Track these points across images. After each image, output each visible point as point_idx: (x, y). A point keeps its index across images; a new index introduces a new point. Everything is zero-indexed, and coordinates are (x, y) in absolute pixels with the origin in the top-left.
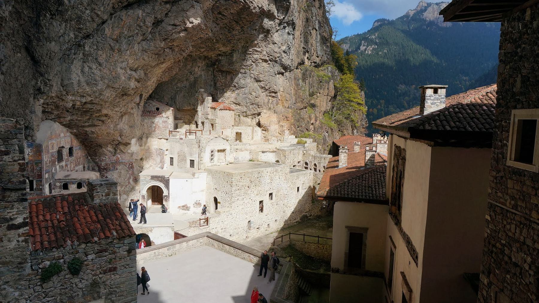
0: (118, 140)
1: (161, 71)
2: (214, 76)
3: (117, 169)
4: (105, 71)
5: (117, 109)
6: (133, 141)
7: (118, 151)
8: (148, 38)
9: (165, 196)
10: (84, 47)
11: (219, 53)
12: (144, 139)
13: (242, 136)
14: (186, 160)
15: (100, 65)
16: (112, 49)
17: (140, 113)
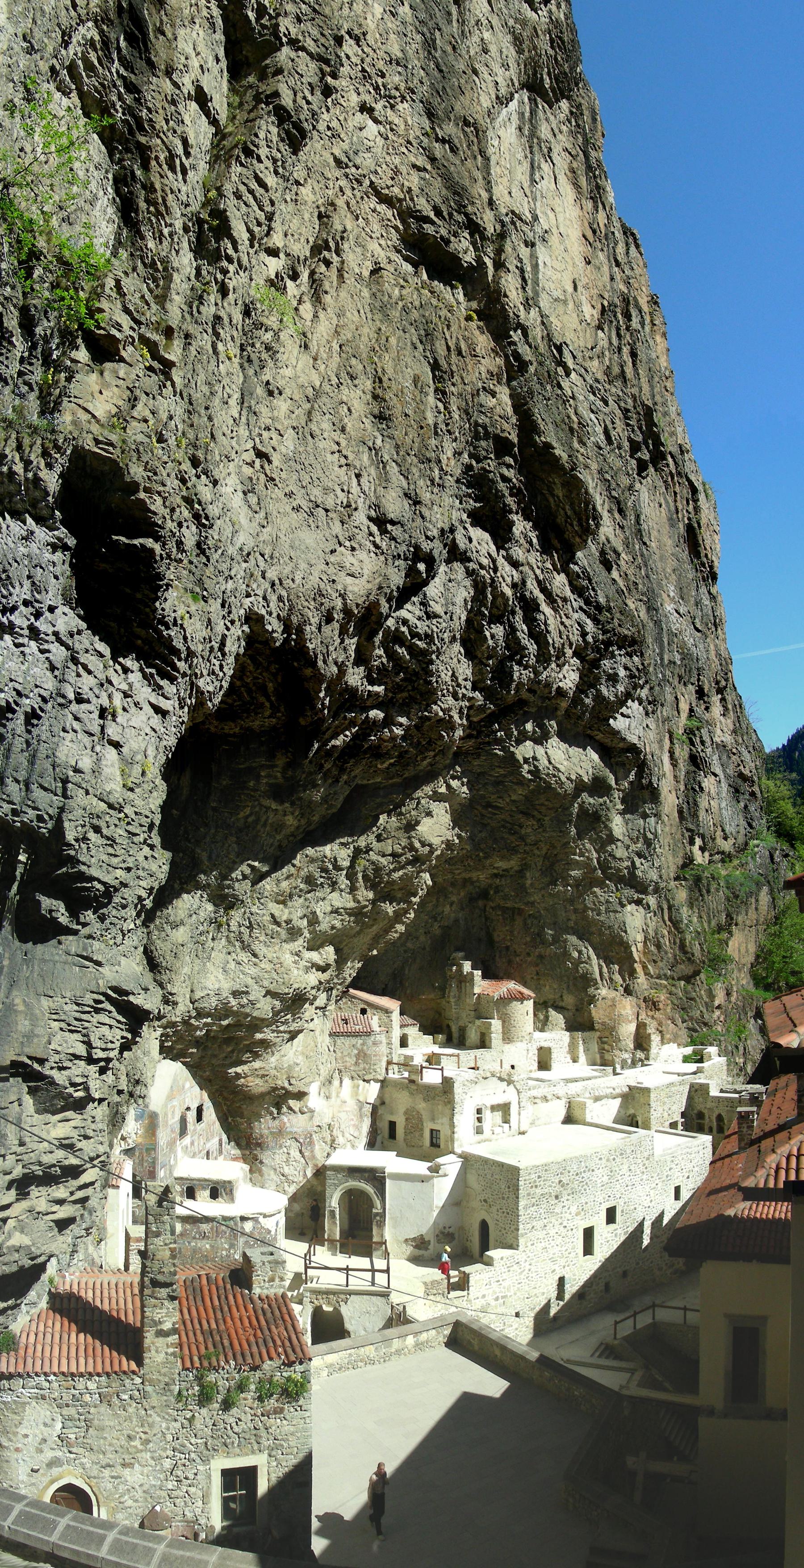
0: (283, 1088)
1: (370, 936)
2: (487, 919)
3: (281, 1147)
4: (263, 966)
5: (282, 1028)
6: (313, 1089)
7: (285, 1109)
8: (343, 887)
9: (377, 1214)
10: (229, 925)
11: (495, 871)
12: (336, 1082)
13: (554, 1056)
14: (422, 1130)
15: (255, 955)
16: (275, 922)
17: (329, 1025)
